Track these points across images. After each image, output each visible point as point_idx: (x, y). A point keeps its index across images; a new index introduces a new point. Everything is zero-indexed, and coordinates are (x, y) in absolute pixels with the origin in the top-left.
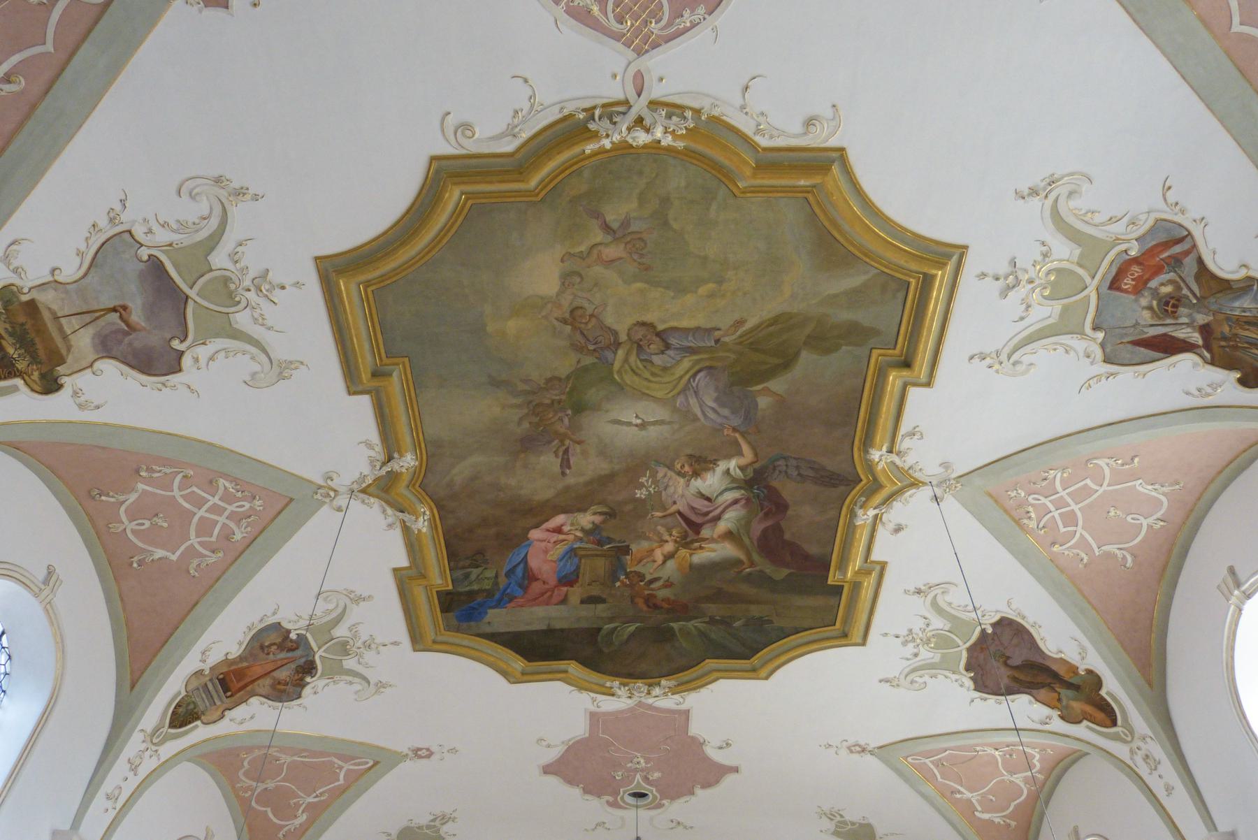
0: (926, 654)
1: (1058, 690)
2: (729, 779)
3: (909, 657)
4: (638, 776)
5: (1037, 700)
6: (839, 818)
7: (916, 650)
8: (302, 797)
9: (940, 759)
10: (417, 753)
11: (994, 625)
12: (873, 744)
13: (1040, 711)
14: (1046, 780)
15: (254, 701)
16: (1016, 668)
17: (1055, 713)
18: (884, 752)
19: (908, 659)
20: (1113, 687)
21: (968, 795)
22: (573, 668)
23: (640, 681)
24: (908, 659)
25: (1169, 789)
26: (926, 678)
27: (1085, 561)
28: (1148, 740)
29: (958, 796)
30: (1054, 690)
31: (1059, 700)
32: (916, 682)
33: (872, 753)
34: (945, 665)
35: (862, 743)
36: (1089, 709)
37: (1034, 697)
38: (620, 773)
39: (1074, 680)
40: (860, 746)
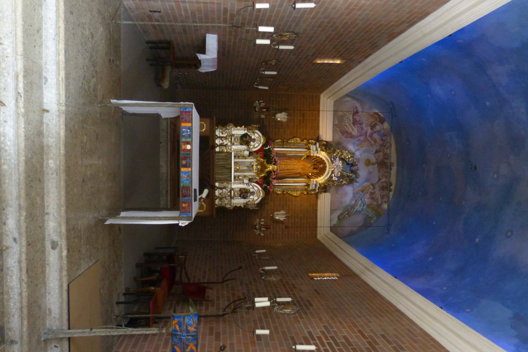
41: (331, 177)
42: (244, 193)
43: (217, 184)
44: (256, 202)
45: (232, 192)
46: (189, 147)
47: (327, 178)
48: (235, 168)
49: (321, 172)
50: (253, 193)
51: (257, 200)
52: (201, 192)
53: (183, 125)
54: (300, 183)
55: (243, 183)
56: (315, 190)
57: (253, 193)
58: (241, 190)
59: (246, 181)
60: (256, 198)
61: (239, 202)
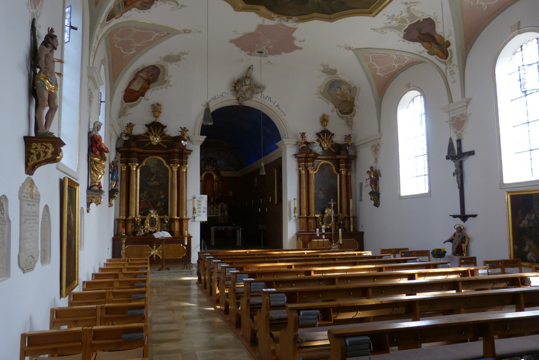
0: (394, 23)
1: (432, 44)
2: (296, 52)
3: (387, 23)
4: (264, 47)
5: (423, 45)
6: (327, 67)
7: (391, 22)
8: (135, 44)
9: (374, 56)
10: (185, 31)
11: (424, 20)
12: (355, 47)
13: (422, 48)
14: (405, 67)
15: (133, 9)
16: (423, 34)
17: (426, 51)
18: (357, 51)
19: (386, 24)
20: (453, 48)
21: (377, 67)
22: (263, 9)
23: (285, 16)
24: (386, 24)
25: (454, 82)
26: (388, 31)
27: (471, 6)
28: (455, 66)
29: (374, 67)
30: (431, 44)
31: (431, 47)
32: (384, 31)
33: (352, 50)
34: (398, 28)
35: (351, 47)
36: (440, 52)
37: (422, 44)
38: (258, 45)
39: (440, 43)
40: (349, 47)
41: (213, 171)
42: (222, 211)
43: (219, 222)
44: (226, 205)
45: (222, 216)
46: (224, 228)
47: (214, 173)
48: (212, 215)
49: (211, 176)
50: (222, 207)
51: (225, 205)
52: (233, 226)
53: (219, 229)
54: (216, 184)
55: (218, 211)
56: (219, 178)
57: (222, 207)
58: (221, 212)
59: (217, 210)
60: (224, 206)
61: (226, 213)
